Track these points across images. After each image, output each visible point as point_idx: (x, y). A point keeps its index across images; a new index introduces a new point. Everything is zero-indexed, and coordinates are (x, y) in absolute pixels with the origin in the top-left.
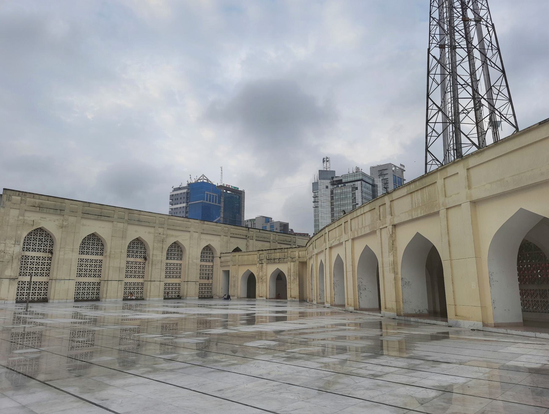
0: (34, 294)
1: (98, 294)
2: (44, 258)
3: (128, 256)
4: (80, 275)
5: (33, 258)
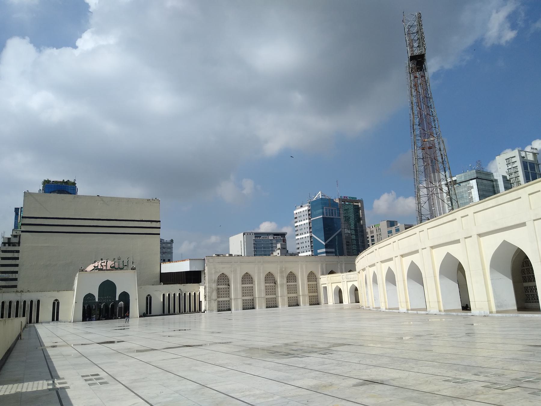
0: (224, 307)
1: (253, 305)
3: (266, 283)
5: (221, 289)
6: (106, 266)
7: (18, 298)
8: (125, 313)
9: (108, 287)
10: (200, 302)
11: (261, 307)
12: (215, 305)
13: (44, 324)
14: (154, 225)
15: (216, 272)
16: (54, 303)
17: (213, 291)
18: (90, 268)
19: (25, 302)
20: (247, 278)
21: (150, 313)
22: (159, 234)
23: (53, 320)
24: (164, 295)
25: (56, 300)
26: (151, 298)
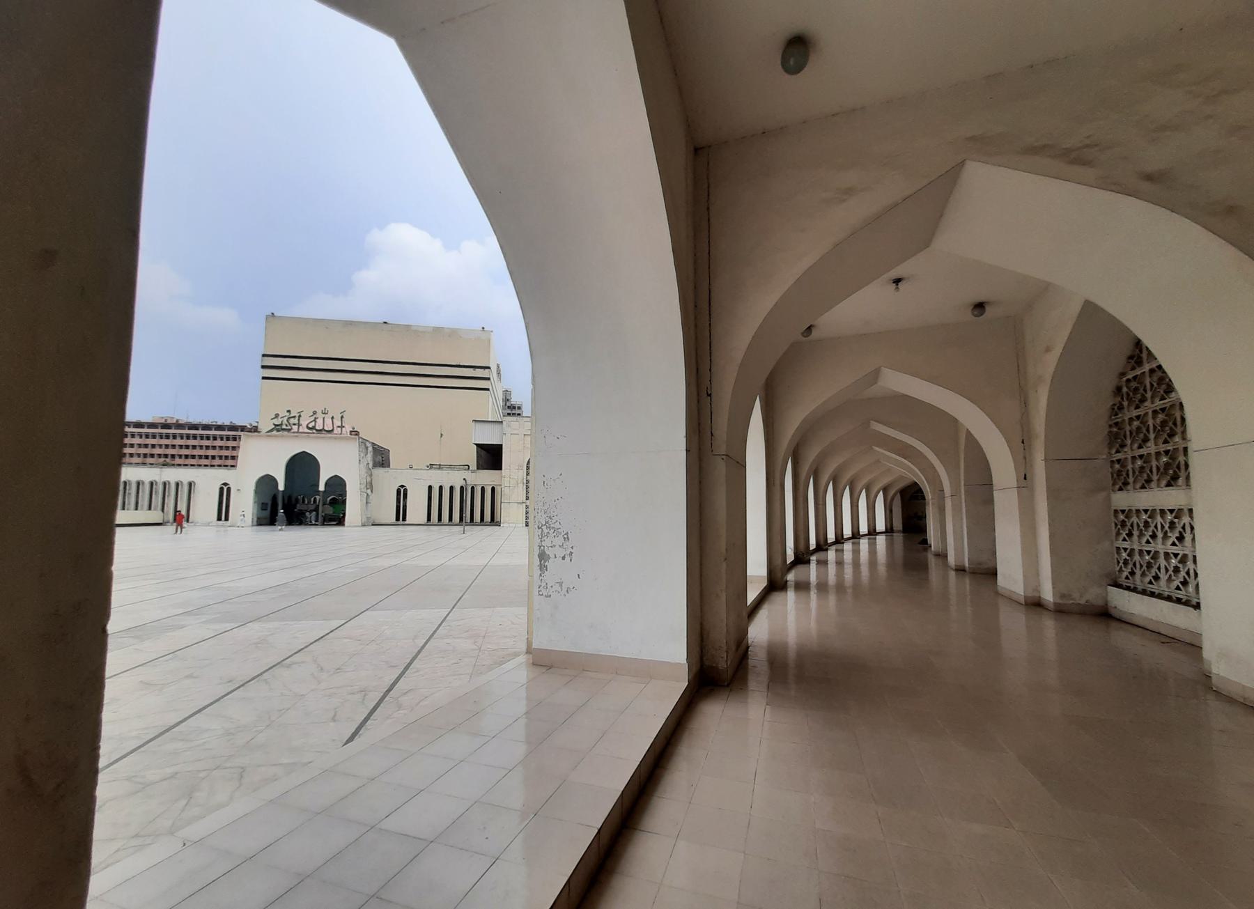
6: (299, 425)
7: (165, 479)
8: (337, 519)
9: (302, 466)
14: (479, 373)
16: (221, 489)
21: (404, 519)
23: (219, 519)
24: (430, 487)
25: (225, 484)
26: (405, 491)
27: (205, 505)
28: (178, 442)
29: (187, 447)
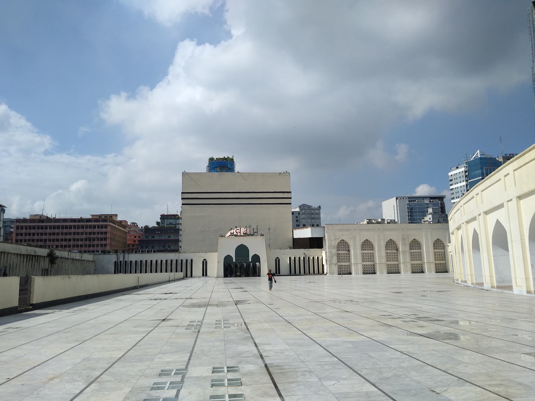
1: (374, 270)
2: (346, 254)
4: (364, 261)
5: (342, 254)
6: (240, 232)
9: (242, 250)
10: (323, 265)
11: (382, 273)
12: (335, 269)
13: (196, 279)
14: (286, 195)
15: (336, 239)
16: (203, 262)
17: (333, 256)
18: (229, 234)
19: (182, 260)
20: (367, 245)
21: (279, 273)
22: (290, 204)
23: (203, 275)
24: (290, 258)
26: (279, 260)
27: (197, 269)
28: (48, 231)
29: (54, 234)
